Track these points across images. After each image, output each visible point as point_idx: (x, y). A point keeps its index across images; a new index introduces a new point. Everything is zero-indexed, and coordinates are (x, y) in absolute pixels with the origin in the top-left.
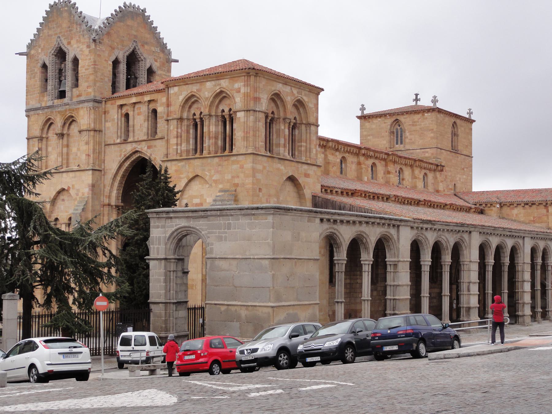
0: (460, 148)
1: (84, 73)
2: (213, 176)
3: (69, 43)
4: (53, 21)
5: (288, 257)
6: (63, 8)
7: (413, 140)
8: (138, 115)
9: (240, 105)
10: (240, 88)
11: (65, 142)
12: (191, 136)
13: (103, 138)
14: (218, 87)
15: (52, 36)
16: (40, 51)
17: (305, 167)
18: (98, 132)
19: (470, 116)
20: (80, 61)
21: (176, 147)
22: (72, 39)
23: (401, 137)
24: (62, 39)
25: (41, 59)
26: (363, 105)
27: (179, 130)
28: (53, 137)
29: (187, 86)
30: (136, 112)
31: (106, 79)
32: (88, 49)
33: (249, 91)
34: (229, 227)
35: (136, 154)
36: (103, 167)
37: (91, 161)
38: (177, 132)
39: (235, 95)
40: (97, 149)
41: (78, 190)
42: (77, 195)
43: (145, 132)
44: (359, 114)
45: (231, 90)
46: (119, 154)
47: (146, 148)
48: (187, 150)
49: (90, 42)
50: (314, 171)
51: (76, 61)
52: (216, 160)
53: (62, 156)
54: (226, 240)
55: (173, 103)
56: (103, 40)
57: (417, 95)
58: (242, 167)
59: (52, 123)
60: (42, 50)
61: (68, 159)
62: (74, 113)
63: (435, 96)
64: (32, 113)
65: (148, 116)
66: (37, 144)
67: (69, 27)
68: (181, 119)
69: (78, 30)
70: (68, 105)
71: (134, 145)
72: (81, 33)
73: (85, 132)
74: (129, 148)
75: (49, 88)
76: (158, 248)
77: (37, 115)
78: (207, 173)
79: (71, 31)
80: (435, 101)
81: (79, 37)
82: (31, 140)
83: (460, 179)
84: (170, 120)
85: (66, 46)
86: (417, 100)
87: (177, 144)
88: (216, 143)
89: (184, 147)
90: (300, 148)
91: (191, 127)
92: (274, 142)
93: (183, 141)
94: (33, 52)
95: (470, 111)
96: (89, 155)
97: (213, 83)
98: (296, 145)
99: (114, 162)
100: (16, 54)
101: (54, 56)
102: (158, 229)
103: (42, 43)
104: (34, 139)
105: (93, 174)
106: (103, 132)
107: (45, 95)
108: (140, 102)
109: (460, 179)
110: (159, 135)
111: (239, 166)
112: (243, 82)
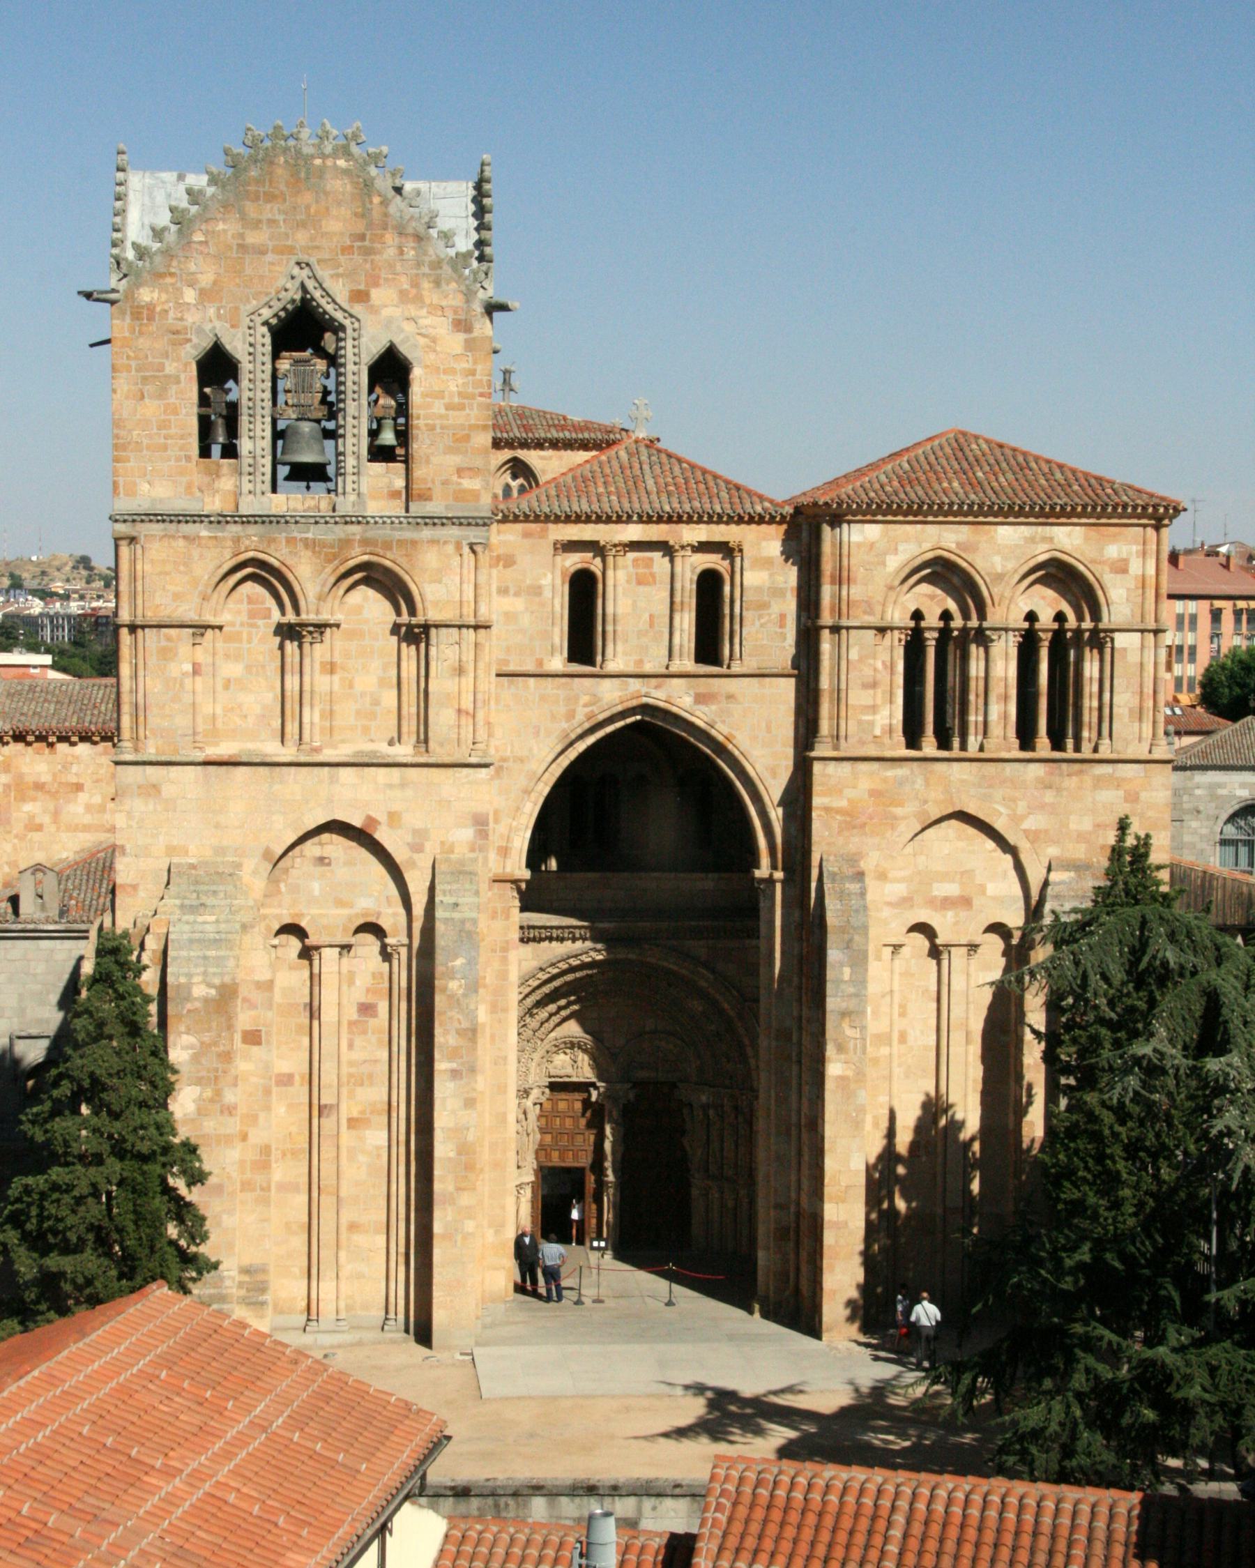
1: (441, 417)
2: (1023, 818)
3: (360, 296)
4: (270, 198)
8: (639, 583)
10: (1126, 561)
14: (1046, 547)
16: (190, 296)
20: (417, 373)
22: (375, 282)
24: (324, 273)
25: (200, 331)
29: (919, 526)
32: (461, 337)
39: (1108, 578)
45: (1093, 561)
46: (562, 710)
49: (469, 310)
55: (859, 573)
60: (205, 296)
62: (389, 555)
64: (156, 528)
66: (184, 649)
67: (362, 237)
69: (405, 257)
70: (359, 523)
71: (635, 684)
72: (426, 270)
73: (455, 631)
77: (181, 543)
78: (1002, 810)
79: (368, 252)
81: (415, 284)
84: (848, 628)
85: (345, 305)
94: (146, 295)
99: (537, 733)
101: (265, 330)
104: (173, 632)
108: (665, 548)
111: (1121, 793)
112: (1136, 543)
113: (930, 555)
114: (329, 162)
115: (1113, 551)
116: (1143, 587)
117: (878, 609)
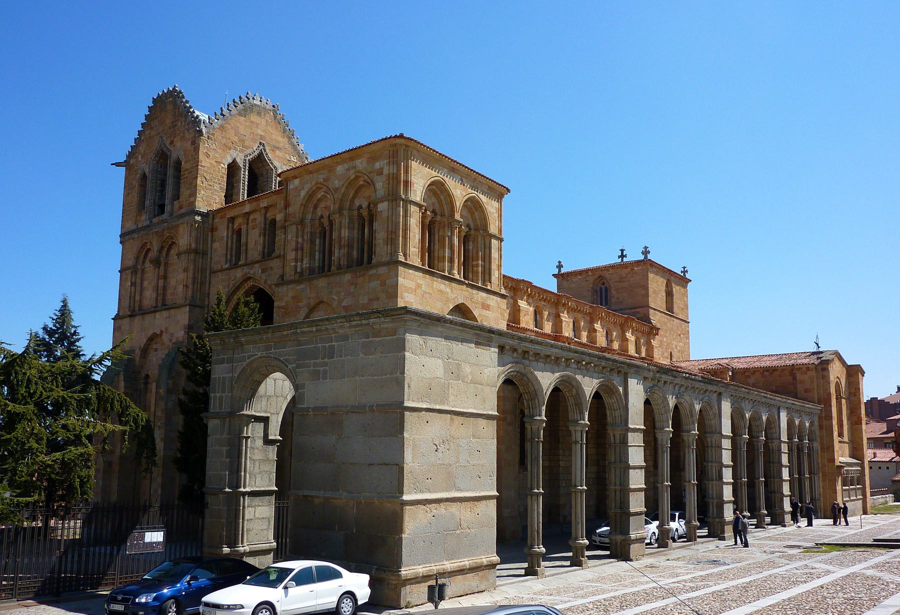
0: (675, 310)
1: (187, 177)
3: (172, 143)
5: (438, 407)
6: (167, 99)
7: (621, 298)
9: (383, 193)
10: (382, 168)
11: (162, 273)
12: (317, 248)
13: (208, 264)
15: (154, 137)
17: (484, 295)
18: (201, 255)
19: (684, 275)
21: (294, 264)
22: (175, 137)
23: (606, 296)
26: (559, 262)
27: (300, 240)
28: (150, 267)
30: (250, 224)
31: (217, 187)
33: (395, 171)
34: (331, 353)
35: (249, 282)
36: (206, 303)
37: (190, 293)
38: (297, 242)
40: (199, 277)
41: (172, 335)
42: (170, 340)
43: (260, 251)
44: (556, 271)
45: (370, 173)
46: (227, 283)
47: (260, 272)
48: (310, 267)
50: (496, 301)
51: (178, 163)
52: (348, 277)
53: (157, 291)
54: (325, 378)
56: (213, 134)
57: (622, 251)
58: (383, 284)
59: (149, 250)
61: (164, 295)
62: (173, 232)
63: (645, 246)
65: (265, 229)
67: (173, 122)
68: (302, 222)
71: (246, 270)
74: (239, 273)
75: (147, 203)
76: (221, 398)
79: (176, 125)
80: (646, 252)
82: (124, 273)
83: (676, 346)
85: (169, 147)
86: (622, 256)
87: (296, 260)
88: (349, 255)
89: (306, 264)
90: (475, 269)
91: (318, 235)
92: (436, 254)
93: (305, 254)
94: (132, 161)
95: (684, 269)
96: (187, 286)
97: (346, 166)
98: (470, 265)
100: (112, 164)
102: (222, 366)
103: (142, 149)
104: (127, 272)
105: (190, 311)
106: (209, 256)
107: (143, 213)
109: (676, 346)
110: (277, 252)
112: (386, 159)
113: (314, 188)
114: (168, 101)
115: (377, 165)
116: (389, 180)
117: (297, 215)
